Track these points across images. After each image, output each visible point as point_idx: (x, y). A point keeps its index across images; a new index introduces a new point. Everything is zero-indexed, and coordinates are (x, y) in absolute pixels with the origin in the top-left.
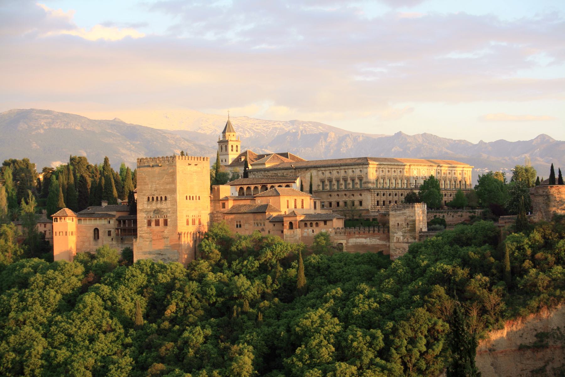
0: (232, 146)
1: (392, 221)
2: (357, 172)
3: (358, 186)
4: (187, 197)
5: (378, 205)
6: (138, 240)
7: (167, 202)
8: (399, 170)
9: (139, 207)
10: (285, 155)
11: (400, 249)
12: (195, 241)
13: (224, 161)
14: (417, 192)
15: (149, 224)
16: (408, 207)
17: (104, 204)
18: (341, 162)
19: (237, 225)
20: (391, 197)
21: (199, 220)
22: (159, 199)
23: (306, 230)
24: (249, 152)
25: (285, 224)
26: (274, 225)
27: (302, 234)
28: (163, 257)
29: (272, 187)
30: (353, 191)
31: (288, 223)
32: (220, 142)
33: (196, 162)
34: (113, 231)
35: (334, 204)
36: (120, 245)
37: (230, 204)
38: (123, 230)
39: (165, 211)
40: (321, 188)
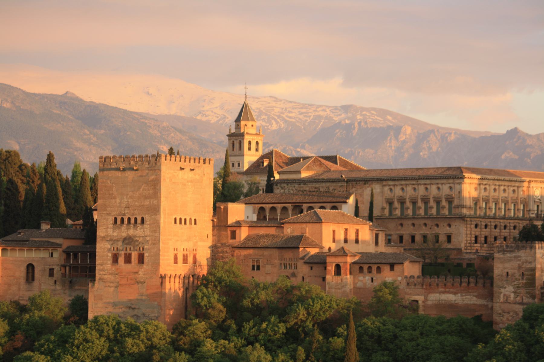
0: (250, 143)
1: (498, 269)
2: (445, 189)
3: (446, 212)
4: (175, 219)
5: (476, 242)
6: (96, 285)
7: (145, 226)
8: (511, 189)
9: (100, 232)
10: (333, 159)
11: (509, 313)
12: (186, 289)
13: (236, 165)
14: (539, 223)
15: (115, 259)
16: (524, 247)
17: (45, 227)
18: (420, 173)
19: (253, 267)
20: (498, 230)
21: (195, 256)
22: (132, 221)
23: (361, 278)
24: (276, 152)
25: (329, 268)
26: (312, 268)
27: (355, 283)
28: (136, 312)
29: (311, 208)
30: (439, 219)
31: (334, 265)
32: (230, 136)
33: (192, 165)
34: (56, 269)
35: (406, 238)
36: (67, 291)
37: (244, 233)
38: (73, 268)
39: (141, 240)
40: (387, 212)
